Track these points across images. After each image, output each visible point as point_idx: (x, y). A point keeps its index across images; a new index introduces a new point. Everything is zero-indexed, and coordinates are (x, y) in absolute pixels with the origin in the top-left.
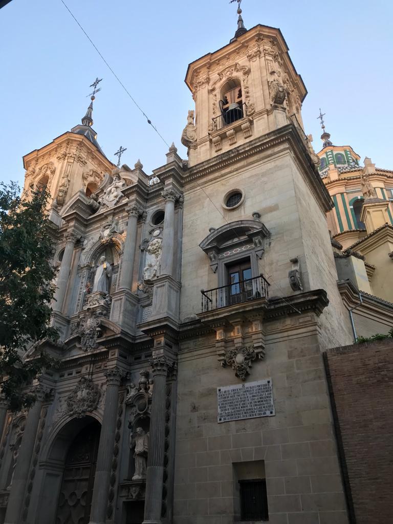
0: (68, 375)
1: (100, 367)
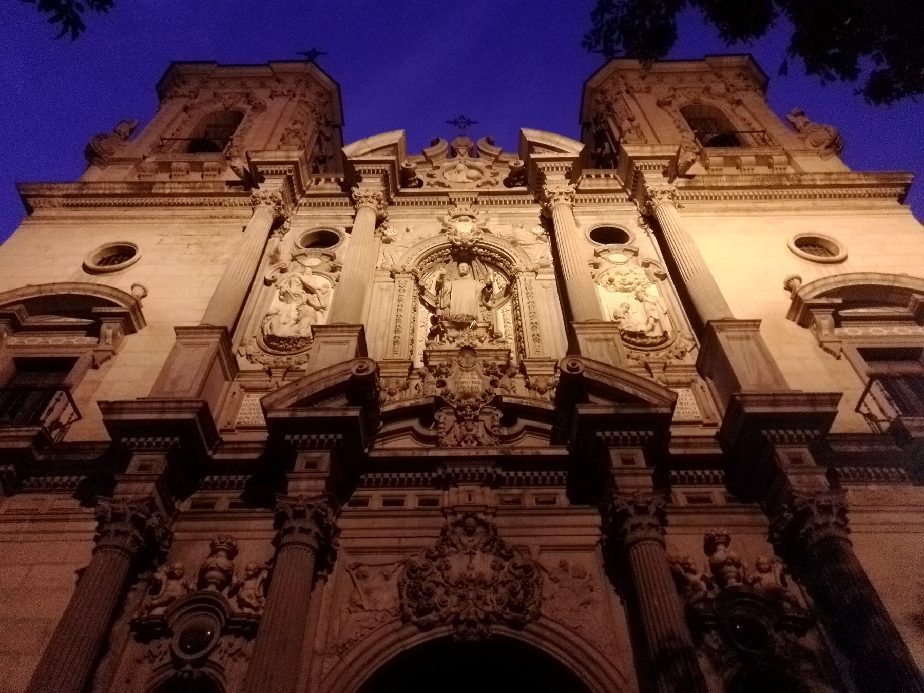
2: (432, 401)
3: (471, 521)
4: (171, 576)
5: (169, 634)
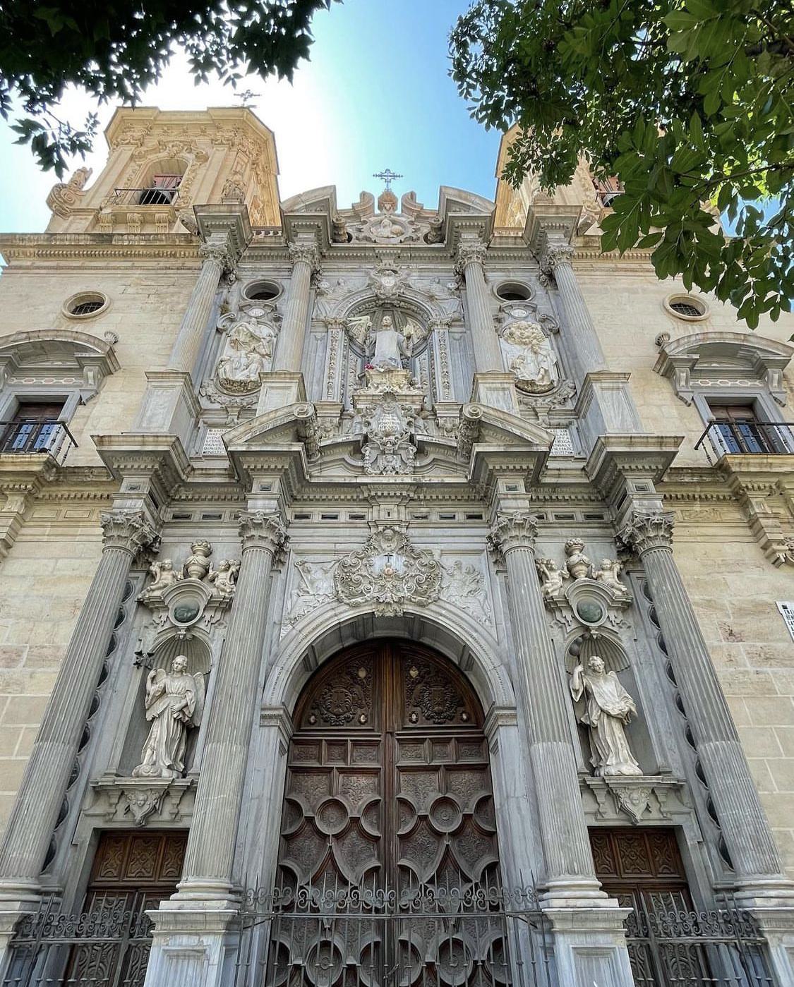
0: (323, 517)
1: (425, 517)
2: (360, 438)
3: (389, 532)
4: (162, 568)
5: (166, 608)
